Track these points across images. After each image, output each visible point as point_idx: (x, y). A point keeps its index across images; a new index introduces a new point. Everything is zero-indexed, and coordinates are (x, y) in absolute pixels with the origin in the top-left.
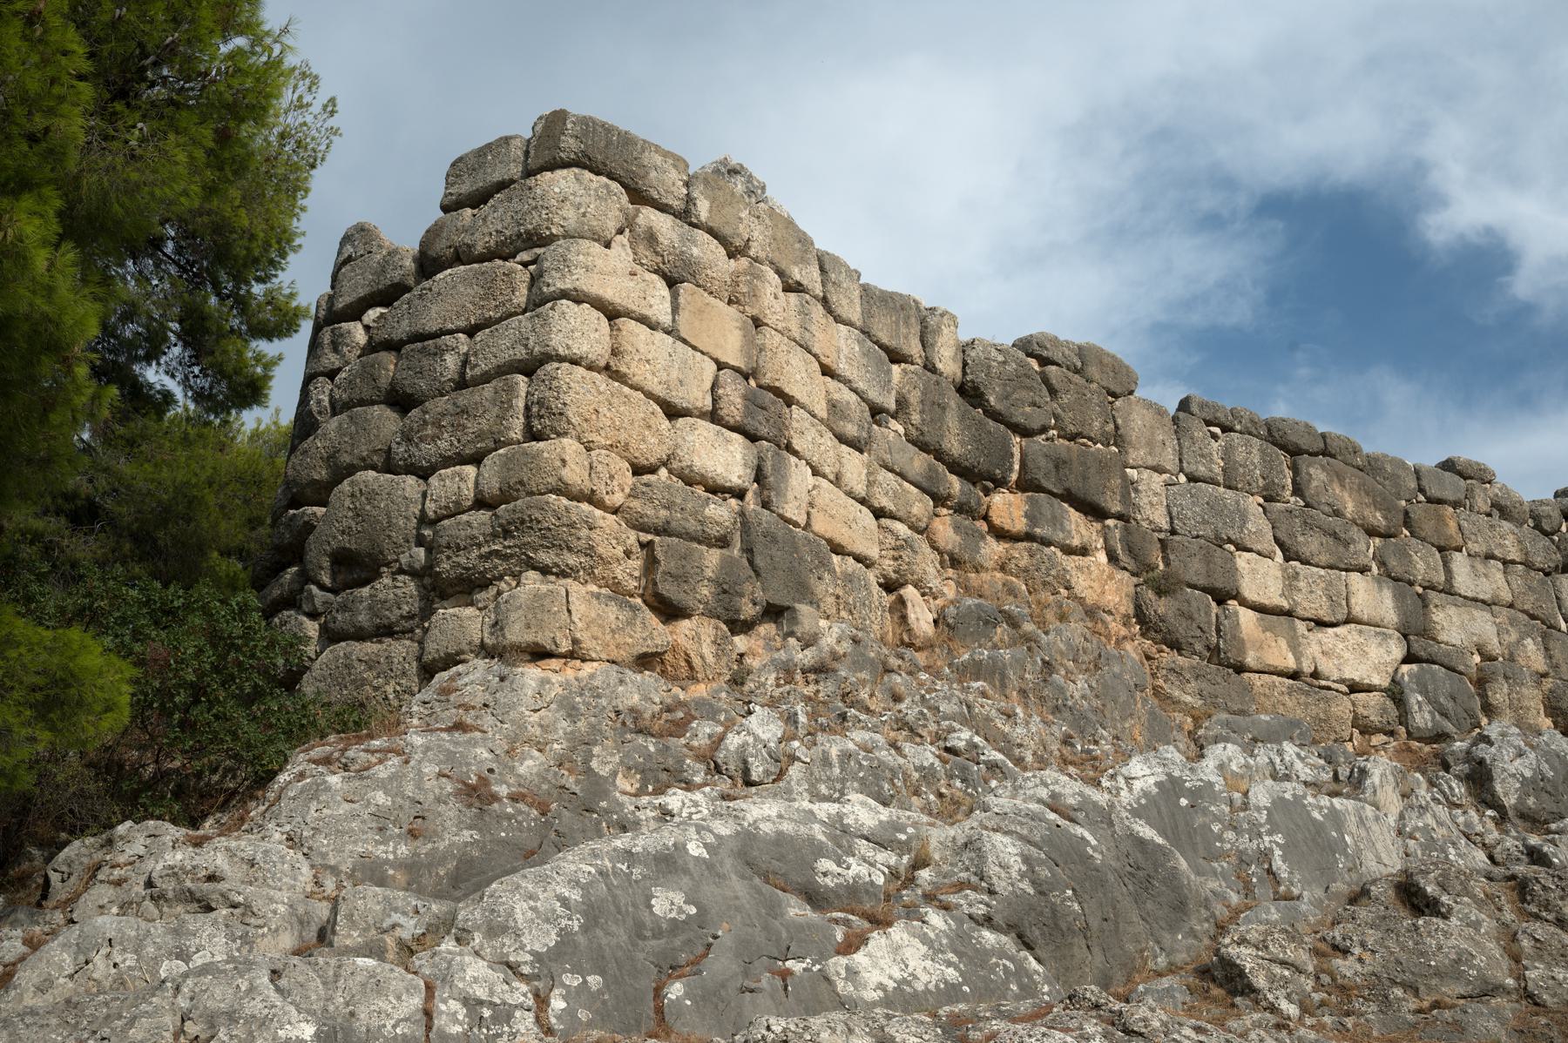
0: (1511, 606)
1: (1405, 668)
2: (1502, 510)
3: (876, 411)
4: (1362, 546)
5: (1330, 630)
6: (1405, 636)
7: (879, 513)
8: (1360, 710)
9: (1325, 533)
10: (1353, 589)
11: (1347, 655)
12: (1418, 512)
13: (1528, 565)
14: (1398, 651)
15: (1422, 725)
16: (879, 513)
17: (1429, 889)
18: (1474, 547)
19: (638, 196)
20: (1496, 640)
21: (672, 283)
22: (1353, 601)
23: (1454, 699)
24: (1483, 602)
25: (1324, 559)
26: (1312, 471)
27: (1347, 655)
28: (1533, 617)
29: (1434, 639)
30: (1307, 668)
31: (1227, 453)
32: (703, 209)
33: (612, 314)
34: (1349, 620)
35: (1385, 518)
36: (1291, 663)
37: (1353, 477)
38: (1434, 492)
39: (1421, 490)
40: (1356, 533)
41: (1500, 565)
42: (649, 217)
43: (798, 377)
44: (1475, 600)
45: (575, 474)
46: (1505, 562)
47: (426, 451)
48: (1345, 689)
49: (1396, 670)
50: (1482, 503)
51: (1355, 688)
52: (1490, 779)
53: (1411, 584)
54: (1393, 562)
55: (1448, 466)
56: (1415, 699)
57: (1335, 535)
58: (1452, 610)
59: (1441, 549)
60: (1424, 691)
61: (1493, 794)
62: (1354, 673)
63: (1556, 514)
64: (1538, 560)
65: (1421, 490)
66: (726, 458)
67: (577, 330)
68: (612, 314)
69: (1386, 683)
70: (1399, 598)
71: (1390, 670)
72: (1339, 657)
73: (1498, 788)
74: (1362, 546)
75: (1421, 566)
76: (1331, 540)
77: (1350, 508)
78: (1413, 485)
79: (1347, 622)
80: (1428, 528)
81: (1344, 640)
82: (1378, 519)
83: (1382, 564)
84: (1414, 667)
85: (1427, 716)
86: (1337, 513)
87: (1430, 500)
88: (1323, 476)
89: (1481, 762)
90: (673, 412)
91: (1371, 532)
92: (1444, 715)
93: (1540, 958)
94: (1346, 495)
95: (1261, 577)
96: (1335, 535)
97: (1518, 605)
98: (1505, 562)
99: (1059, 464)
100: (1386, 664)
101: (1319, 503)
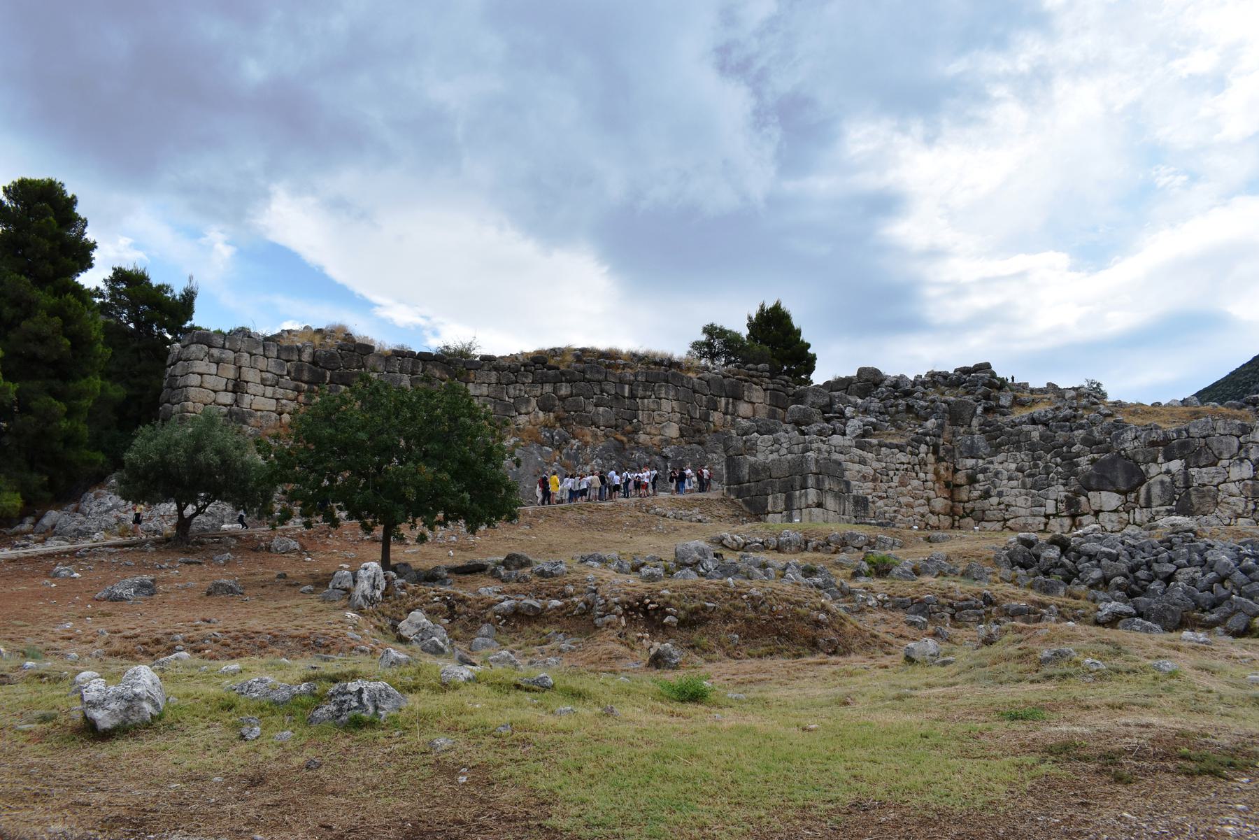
3: (281, 376)
7: (277, 399)
16: (277, 399)
19: (210, 347)
21: (218, 364)
31: (401, 364)
32: (227, 345)
33: (201, 374)
42: (214, 351)
43: (250, 375)
45: (191, 409)
66: (227, 398)
67: (195, 380)
68: (201, 374)
77: (438, 375)
90: (215, 392)
99: (341, 376)
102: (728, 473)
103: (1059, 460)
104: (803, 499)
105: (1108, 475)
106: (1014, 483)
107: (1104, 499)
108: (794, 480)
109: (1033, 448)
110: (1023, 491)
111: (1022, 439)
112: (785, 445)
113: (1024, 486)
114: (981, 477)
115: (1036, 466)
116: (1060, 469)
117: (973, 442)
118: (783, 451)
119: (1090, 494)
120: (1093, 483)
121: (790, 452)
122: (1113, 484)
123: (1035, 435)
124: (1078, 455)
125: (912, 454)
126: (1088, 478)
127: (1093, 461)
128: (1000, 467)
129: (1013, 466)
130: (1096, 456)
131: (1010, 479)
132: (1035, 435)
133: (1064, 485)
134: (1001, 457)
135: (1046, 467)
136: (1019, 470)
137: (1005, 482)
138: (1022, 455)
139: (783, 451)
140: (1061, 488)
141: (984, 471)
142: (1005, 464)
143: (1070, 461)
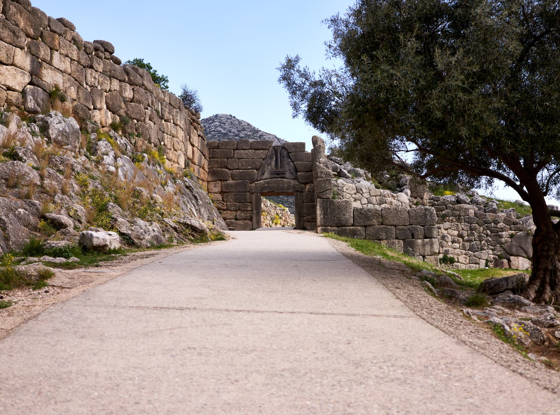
0: (70, 74)
1: (29, 86)
2: (75, 41)
4: (23, 40)
5: (5, 66)
6: (31, 75)
8: (9, 97)
9: (11, 31)
10: (16, 54)
11: (9, 76)
12: (46, 33)
13: (79, 62)
14: (27, 80)
15: (30, 107)
17: (20, 154)
18: (63, 52)
20: (62, 85)
22: (15, 58)
23: (43, 101)
24: (61, 71)
25: (8, 40)
26: (11, 7)
27: (9, 76)
28: (76, 80)
29: (41, 79)
34: (13, 64)
35: (34, 32)
37: (26, 14)
38: (54, 28)
39: (49, 26)
40: (22, 34)
41: (70, 60)
44: (58, 69)
46: (71, 59)
48: (5, 88)
49: (25, 87)
50: (69, 37)
51: (9, 89)
52: (48, 128)
53: (38, 58)
54: (33, 49)
55: (61, 20)
56: (29, 97)
57: (14, 33)
58: (50, 71)
59: (51, 49)
60: (33, 96)
61: (48, 133)
62: (10, 83)
63: (92, 48)
64: (83, 62)
65: (49, 26)
69: (21, 90)
70: (32, 62)
71: (23, 86)
72: (6, 77)
73: (50, 132)
74: (23, 40)
75: (42, 53)
76: (12, 34)
77: (22, 24)
78: (47, 23)
79: (12, 65)
80: (48, 40)
81: (9, 71)
82: (31, 32)
83: (29, 48)
84: (32, 87)
85: (33, 104)
86: (17, 25)
87: (51, 31)
88: (15, 10)
89: (47, 122)
91: (28, 36)
92: (38, 105)
93: (49, 178)
94: (22, 20)
96: (14, 33)
97: (72, 74)
98: (71, 59)
100: (22, 83)
101: (11, 19)
102: (325, 214)
103: (489, 232)
104: (428, 248)
105: (523, 246)
106: (457, 245)
107: (521, 262)
108: (416, 229)
109: (469, 221)
110: (464, 252)
111: (462, 214)
112: (366, 195)
113: (464, 248)
115: (472, 234)
119: (512, 258)
120: (514, 250)
121: (369, 202)
122: (526, 252)
123: (471, 212)
124: (502, 230)
126: (511, 246)
127: (512, 236)
128: (445, 232)
129: (456, 233)
130: (513, 232)
131: (453, 242)
132: (471, 212)
133: (493, 250)
134: (447, 225)
135: (480, 237)
136: (460, 236)
137: (450, 244)
138: (462, 226)
139: (365, 201)
140: (491, 252)
142: (450, 231)
143: (496, 233)
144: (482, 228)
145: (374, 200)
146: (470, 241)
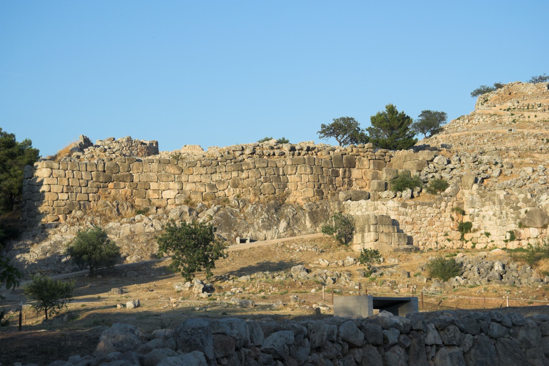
7: (88, 194)
30: (160, 197)
36: (158, 197)
47: (35, 199)
82: (178, 172)
95: (153, 186)
106: (492, 222)
107: (531, 232)
110: (496, 227)
112: (364, 207)
114: (476, 218)
115: (501, 213)
116: (513, 215)
117: (473, 199)
118: (364, 210)
120: (526, 223)
124: (520, 208)
125: (437, 207)
134: (486, 208)
135: (507, 214)
136: (494, 215)
139: (364, 210)
141: (478, 215)
144: (508, 208)
145: (370, 209)
146: (500, 218)
